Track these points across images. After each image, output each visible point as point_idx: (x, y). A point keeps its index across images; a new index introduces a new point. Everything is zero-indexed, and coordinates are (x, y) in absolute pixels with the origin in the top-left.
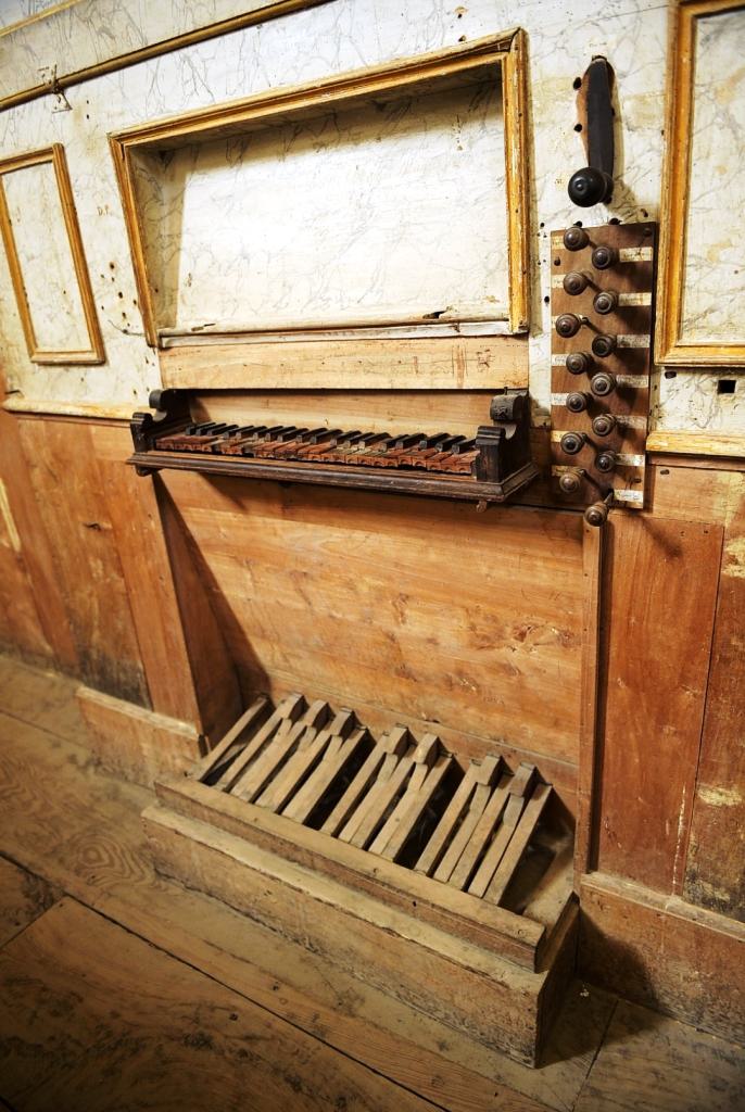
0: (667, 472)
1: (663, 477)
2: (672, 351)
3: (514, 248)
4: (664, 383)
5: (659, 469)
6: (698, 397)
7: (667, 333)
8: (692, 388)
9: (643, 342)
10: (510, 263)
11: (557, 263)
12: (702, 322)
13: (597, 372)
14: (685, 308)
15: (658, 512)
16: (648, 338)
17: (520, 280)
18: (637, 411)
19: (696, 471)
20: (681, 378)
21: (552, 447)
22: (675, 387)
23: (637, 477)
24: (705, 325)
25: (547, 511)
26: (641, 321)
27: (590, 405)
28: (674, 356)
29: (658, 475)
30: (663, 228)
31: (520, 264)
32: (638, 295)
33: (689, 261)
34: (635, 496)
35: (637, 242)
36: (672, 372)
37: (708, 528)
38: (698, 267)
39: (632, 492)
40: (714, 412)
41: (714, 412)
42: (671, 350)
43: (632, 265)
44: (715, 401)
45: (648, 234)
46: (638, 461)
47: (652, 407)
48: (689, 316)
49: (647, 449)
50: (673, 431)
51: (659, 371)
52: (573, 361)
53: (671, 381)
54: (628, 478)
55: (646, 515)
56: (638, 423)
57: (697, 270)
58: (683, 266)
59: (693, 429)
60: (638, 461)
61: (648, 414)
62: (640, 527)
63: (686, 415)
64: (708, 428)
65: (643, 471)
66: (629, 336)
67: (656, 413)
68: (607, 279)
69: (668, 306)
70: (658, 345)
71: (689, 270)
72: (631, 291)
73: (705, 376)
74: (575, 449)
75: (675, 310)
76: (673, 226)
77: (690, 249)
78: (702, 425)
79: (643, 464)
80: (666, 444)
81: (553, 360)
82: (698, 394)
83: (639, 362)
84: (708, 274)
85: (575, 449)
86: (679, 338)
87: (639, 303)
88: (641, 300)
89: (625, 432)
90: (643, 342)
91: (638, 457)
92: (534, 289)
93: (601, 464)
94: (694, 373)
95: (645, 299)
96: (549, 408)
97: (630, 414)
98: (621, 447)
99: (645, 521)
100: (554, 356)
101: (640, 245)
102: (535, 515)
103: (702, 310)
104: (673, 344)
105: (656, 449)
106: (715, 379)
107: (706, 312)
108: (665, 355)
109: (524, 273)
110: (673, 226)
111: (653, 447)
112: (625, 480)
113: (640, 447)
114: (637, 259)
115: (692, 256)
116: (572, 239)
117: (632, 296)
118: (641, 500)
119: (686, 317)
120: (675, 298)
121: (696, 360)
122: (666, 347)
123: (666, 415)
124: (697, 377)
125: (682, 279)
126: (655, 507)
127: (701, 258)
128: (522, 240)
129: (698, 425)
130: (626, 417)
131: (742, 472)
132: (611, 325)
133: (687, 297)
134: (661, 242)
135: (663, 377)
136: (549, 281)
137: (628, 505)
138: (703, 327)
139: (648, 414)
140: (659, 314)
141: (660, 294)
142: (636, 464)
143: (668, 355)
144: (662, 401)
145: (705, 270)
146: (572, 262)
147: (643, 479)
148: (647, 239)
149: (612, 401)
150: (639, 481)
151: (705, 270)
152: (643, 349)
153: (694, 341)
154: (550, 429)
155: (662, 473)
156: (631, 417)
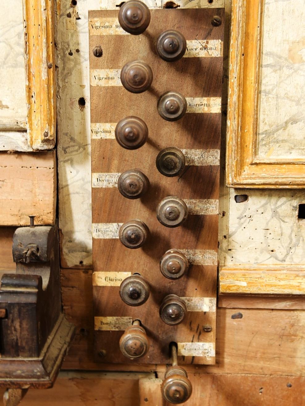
0: (240, 316)
1: (235, 322)
2: (247, 170)
3: (33, 31)
4: (235, 208)
5: (229, 313)
6: (275, 223)
7: (241, 146)
8: (268, 214)
9: (212, 158)
10: (27, 52)
11: (98, 54)
12: (281, 135)
13: (163, 198)
14: (261, 117)
15: (232, 369)
16: (217, 153)
17: (44, 76)
18: (204, 243)
19: (275, 313)
20: (254, 202)
21: (95, 293)
22: (248, 213)
23: (207, 326)
24: (285, 137)
25: (86, 375)
26: (209, 131)
27: (150, 243)
28: (250, 176)
29: (229, 321)
30: (237, 17)
31: (45, 55)
32: (205, 100)
33: (266, 60)
34: (203, 349)
35: (203, 33)
36: (243, 195)
37: (291, 381)
38: (277, 67)
39: (201, 344)
40: (294, 240)
41: (294, 240)
42: (246, 168)
43: (197, 61)
44: (295, 229)
45: (216, 24)
46: (206, 305)
47: (220, 238)
48: (267, 128)
49: (221, 290)
50: (247, 267)
51: (228, 194)
52: (128, 181)
53: (242, 205)
54: (195, 327)
55: (216, 371)
56: (206, 258)
57: (275, 71)
58: (260, 66)
59: (271, 262)
60: (206, 305)
61: (217, 245)
62: (209, 387)
63: (257, 244)
64: (288, 259)
65: (214, 317)
66: (193, 151)
67: (224, 245)
68: (164, 78)
69: (242, 114)
70: (231, 161)
71: (265, 71)
72: (196, 95)
73: (283, 200)
74: (140, 301)
75: (250, 120)
76: (247, 16)
77: (266, 48)
78: (281, 257)
79: (214, 308)
80: (244, 284)
81: (95, 180)
82: (275, 222)
83: (205, 183)
84: (289, 76)
85: (140, 301)
86: (255, 153)
87: (206, 110)
88: (208, 105)
89: (192, 270)
90: (212, 158)
91: (207, 300)
92: (64, 87)
93: (169, 316)
94: (270, 196)
95: (212, 106)
96: (89, 244)
97: (196, 247)
98: (185, 288)
99: (215, 379)
100: (96, 175)
101: (208, 36)
102: (72, 384)
103: (283, 119)
104: (248, 160)
105: (233, 290)
106: (296, 203)
107: (286, 123)
108: (240, 174)
109: (49, 67)
110: (247, 16)
111: (229, 287)
112: (191, 329)
113: (213, 288)
114: (202, 54)
115: (270, 54)
116: (134, 16)
117: (197, 100)
118: (213, 353)
119: (262, 128)
120: (250, 105)
121: (280, 181)
122: (241, 164)
123: (237, 246)
124: (273, 200)
125: (258, 81)
126: (227, 360)
127: (280, 57)
128: (47, 21)
129: (276, 258)
130: (191, 252)
131: (302, 310)
132: (170, 136)
133: (264, 105)
134: (233, 34)
135: (232, 201)
136: (95, 78)
137: (196, 361)
138: (283, 141)
139: (217, 245)
140: (232, 123)
141: (233, 99)
142: (206, 309)
143: (245, 174)
144: (232, 229)
145: (286, 71)
146: (118, 54)
147: (214, 326)
148: (215, 29)
149: (175, 235)
150: (208, 330)
151: (286, 71)
152: (211, 168)
153: (273, 158)
154: (91, 268)
155: (234, 317)
156: (198, 251)
